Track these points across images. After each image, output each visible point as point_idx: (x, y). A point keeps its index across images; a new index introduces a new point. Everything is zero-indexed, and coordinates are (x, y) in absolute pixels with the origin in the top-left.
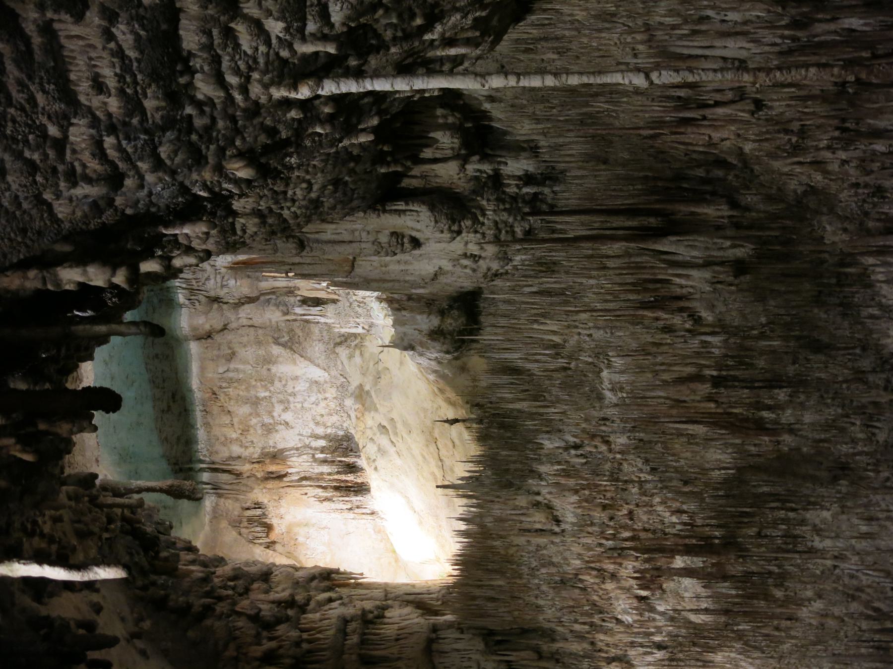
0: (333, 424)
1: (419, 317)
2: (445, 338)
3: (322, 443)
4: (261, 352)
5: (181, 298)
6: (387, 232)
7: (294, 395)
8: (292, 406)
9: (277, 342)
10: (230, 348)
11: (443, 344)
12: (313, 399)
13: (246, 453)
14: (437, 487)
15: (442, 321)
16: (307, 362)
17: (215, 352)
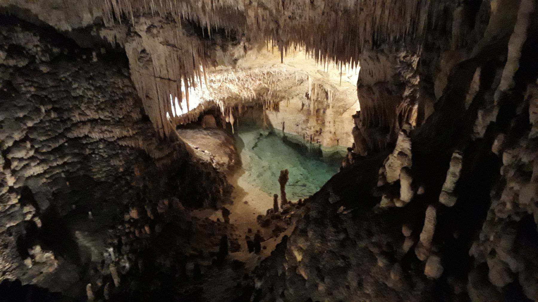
1: (218, 55)
5: (316, 145)
9: (341, 114)
10: (344, 134)
11: (228, 46)
14: (282, 62)
17: (344, 140)
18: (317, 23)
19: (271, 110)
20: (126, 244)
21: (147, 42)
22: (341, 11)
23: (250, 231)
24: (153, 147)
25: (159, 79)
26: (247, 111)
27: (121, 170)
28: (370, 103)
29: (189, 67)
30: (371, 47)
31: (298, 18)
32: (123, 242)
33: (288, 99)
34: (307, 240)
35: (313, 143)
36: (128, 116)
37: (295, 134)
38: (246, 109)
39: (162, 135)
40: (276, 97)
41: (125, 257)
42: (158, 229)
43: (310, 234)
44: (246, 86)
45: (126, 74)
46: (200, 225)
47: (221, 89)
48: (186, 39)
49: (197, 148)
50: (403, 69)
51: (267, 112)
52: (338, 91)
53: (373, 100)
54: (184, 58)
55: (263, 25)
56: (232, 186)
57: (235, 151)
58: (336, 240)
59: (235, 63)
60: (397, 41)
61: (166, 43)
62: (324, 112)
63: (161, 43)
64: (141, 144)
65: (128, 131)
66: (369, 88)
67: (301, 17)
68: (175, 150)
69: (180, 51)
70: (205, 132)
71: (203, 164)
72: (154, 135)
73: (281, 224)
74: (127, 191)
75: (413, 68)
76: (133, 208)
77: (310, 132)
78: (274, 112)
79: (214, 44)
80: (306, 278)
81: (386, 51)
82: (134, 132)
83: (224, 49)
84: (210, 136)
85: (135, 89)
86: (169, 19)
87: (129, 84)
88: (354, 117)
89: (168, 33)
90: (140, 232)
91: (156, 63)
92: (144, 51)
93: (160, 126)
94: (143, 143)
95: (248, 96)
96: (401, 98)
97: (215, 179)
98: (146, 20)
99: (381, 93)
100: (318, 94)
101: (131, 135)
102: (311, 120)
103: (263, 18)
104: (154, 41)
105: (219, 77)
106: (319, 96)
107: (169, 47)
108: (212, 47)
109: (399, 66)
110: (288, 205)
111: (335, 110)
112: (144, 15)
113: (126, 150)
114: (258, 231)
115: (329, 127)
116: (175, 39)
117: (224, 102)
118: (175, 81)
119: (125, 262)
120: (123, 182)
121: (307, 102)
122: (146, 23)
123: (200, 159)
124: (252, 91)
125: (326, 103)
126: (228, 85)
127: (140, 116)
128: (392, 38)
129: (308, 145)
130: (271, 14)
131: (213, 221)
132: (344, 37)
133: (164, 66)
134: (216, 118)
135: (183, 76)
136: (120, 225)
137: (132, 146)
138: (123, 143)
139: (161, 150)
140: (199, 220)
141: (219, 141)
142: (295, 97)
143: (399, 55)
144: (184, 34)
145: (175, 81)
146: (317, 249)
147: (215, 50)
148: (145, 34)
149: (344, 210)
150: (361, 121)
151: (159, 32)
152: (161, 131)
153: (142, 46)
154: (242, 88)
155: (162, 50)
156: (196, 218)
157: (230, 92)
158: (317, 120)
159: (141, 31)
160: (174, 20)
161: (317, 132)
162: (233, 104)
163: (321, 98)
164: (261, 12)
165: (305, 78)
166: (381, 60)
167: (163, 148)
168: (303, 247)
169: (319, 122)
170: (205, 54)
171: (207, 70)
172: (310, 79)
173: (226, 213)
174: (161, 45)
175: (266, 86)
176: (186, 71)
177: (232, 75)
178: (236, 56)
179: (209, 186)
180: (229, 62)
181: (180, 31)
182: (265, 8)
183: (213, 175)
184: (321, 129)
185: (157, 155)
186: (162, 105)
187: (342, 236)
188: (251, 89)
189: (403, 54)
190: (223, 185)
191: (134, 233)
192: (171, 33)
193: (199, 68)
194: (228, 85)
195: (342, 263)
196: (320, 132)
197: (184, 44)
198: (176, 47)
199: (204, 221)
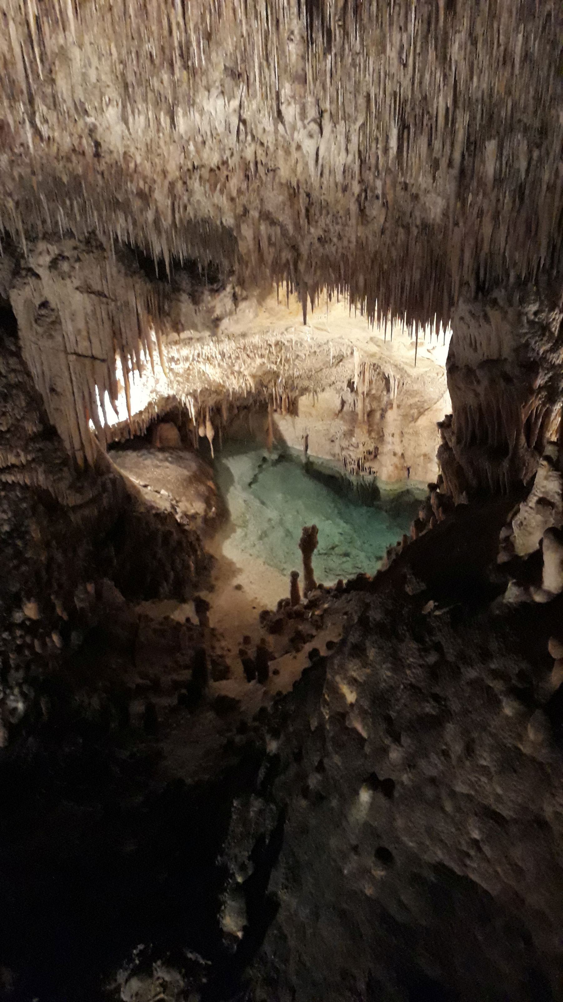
1: (184, 310)
2: (197, 291)
5: (369, 478)
9: (415, 420)
10: (419, 457)
11: (202, 293)
14: (305, 323)
15: (184, 291)
16: (442, 400)
18: (372, 249)
19: (284, 413)
20: (17, 668)
21: (50, 287)
22: (417, 227)
23: (247, 640)
24: (63, 485)
25: (73, 357)
26: (237, 416)
27: (6, 528)
28: (471, 400)
29: (129, 334)
30: (473, 294)
31: (335, 240)
32: (12, 662)
33: (315, 391)
34: (365, 665)
35: (361, 474)
36: (15, 429)
37: (328, 457)
38: (236, 411)
39: (80, 461)
40: (293, 388)
41: (16, 691)
42: (75, 638)
43: (372, 653)
44: (236, 368)
45: (13, 348)
46: (155, 631)
47: (189, 375)
48: (122, 281)
49: (146, 486)
50: (533, 337)
51: (276, 416)
52: (409, 376)
53: (477, 395)
54: (121, 317)
55: (269, 255)
56: (211, 557)
57: (216, 492)
58: (421, 666)
59: (217, 326)
60: (521, 284)
61: (87, 289)
62: (383, 416)
63: (77, 289)
64: (41, 479)
65: (18, 455)
66: (470, 371)
67: (340, 238)
68: (105, 489)
69: (113, 304)
70: (161, 456)
71: (157, 515)
72: (65, 462)
73: (304, 627)
74: (17, 567)
75: (552, 333)
76: (29, 600)
77: (356, 454)
78: (288, 417)
79: (177, 289)
80: (365, 735)
81: (501, 303)
82: (29, 458)
83: (195, 300)
84: (171, 462)
85: (29, 374)
86: (91, 243)
87: (18, 367)
88: (441, 425)
89: (91, 271)
90: (44, 645)
91: (68, 327)
92: (44, 304)
93: (77, 445)
94: (47, 478)
95: (240, 387)
96: (530, 391)
97: (180, 543)
98: (50, 246)
99: (492, 381)
100: (371, 382)
101: (24, 461)
102: (357, 431)
103: (269, 238)
104: (65, 285)
105: (185, 351)
106: (374, 386)
107: (92, 296)
108: (172, 296)
109: (525, 331)
110: (317, 593)
111: (402, 411)
112: (47, 237)
113: (14, 490)
114: (263, 641)
115: (393, 444)
116: (104, 282)
117: (196, 399)
118: (103, 361)
119: (17, 701)
120: (9, 551)
121: (349, 397)
122: (48, 252)
123: (152, 507)
124: (248, 378)
125: (385, 399)
126: (202, 367)
127: (41, 428)
128: (512, 279)
129: (353, 478)
130: (284, 232)
131: (178, 623)
132: (421, 275)
133: (84, 333)
134: (180, 429)
135: (118, 351)
136: (6, 630)
137: (26, 484)
138: (10, 478)
139: (80, 491)
140: (152, 620)
141: (186, 473)
142: (327, 388)
143: (527, 309)
144: (119, 272)
145: (103, 361)
146: (385, 681)
147: (179, 301)
148: (47, 272)
149: (436, 608)
150: (453, 433)
151: (73, 268)
152: (79, 455)
153: (41, 295)
154: (229, 371)
155: (80, 301)
156: (147, 616)
157: (206, 379)
158: (369, 432)
159: (40, 266)
160: (101, 245)
161: (370, 453)
162: (211, 402)
163: (377, 390)
164: (266, 228)
165: (346, 351)
166: (492, 319)
167: (82, 487)
168: (358, 678)
169: (373, 435)
170: (161, 309)
171: (163, 338)
172: (356, 353)
173: (202, 607)
174: (78, 292)
175: (274, 367)
176: (124, 341)
177: (210, 348)
178: (218, 312)
179: (168, 557)
180: (204, 324)
181: (112, 266)
182: (273, 223)
183: (175, 536)
184: (376, 448)
185: (72, 499)
186: (80, 407)
187: (432, 658)
188: (246, 373)
189: (533, 308)
190: (196, 556)
191: (31, 647)
192: (97, 271)
193: (148, 337)
194: (202, 367)
195: (433, 707)
196: (374, 454)
197: (120, 291)
198: (105, 296)
199: (161, 624)
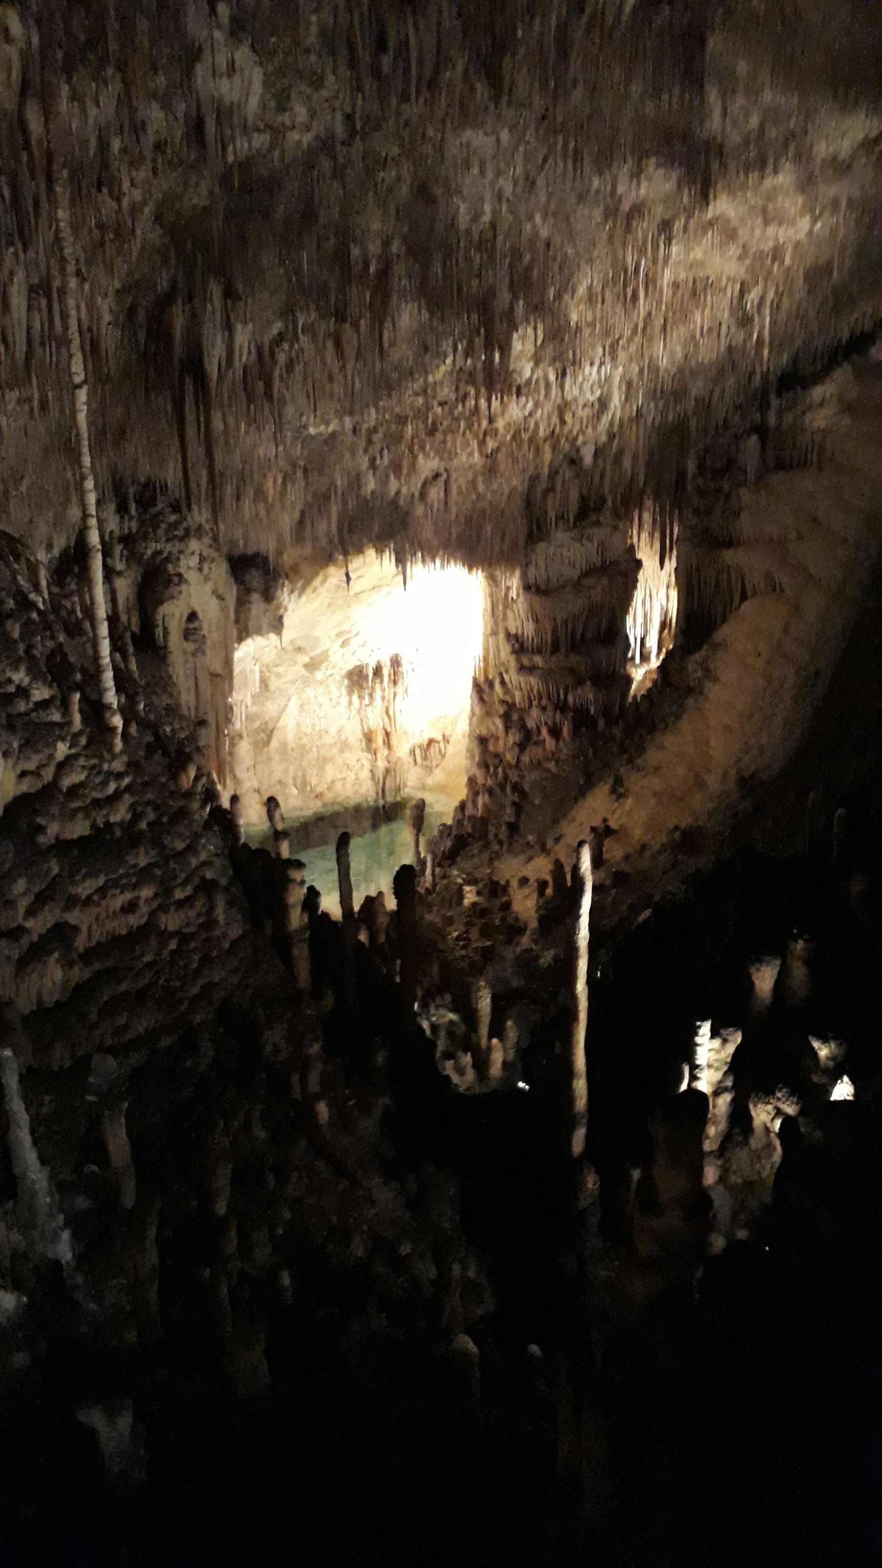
0: (338, 689)
3: (355, 697)
4: (277, 758)
6: (185, 644)
7: (313, 726)
8: (324, 727)
10: (275, 785)
12: (317, 708)
13: (367, 767)
15: (256, 590)
16: (283, 716)
